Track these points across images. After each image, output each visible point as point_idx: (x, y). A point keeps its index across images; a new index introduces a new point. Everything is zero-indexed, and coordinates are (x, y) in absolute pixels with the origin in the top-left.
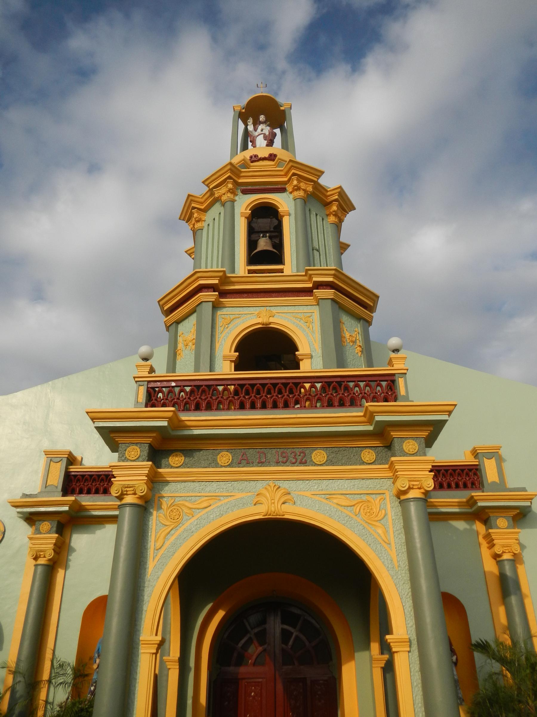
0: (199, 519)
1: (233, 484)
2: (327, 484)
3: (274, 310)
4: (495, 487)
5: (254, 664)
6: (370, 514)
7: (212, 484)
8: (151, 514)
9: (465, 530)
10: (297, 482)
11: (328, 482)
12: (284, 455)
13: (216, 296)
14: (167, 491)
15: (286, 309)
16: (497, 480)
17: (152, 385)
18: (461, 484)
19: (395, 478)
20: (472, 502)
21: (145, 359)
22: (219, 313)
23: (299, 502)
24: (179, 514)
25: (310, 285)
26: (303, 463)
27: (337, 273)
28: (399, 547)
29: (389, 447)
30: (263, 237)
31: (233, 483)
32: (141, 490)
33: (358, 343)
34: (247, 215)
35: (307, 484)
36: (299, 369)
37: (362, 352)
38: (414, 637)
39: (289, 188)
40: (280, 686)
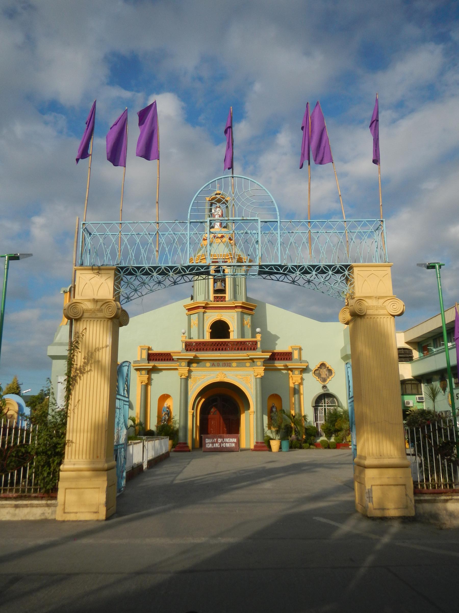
3: (223, 314)
4: (296, 361)
5: (213, 414)
8: (189, 380)
9: (286, 373)
14: (192, 374)
15: (226, 314)
16: (297, 358)
17: (186, 343)
18: (285, 358)
19: (254, 372)
20: (286, 366)
21: (184, 334)
22: (205, 314)
23: (228, 377)
25: (234, 306)
26: (230, 366)
29: (254, 362)
30: (219, 281)
33: (249, 324)
36: (230, 338)
37: (250, 327)
38: (255, 411)
39: (229, 262)
40: (222, 421)
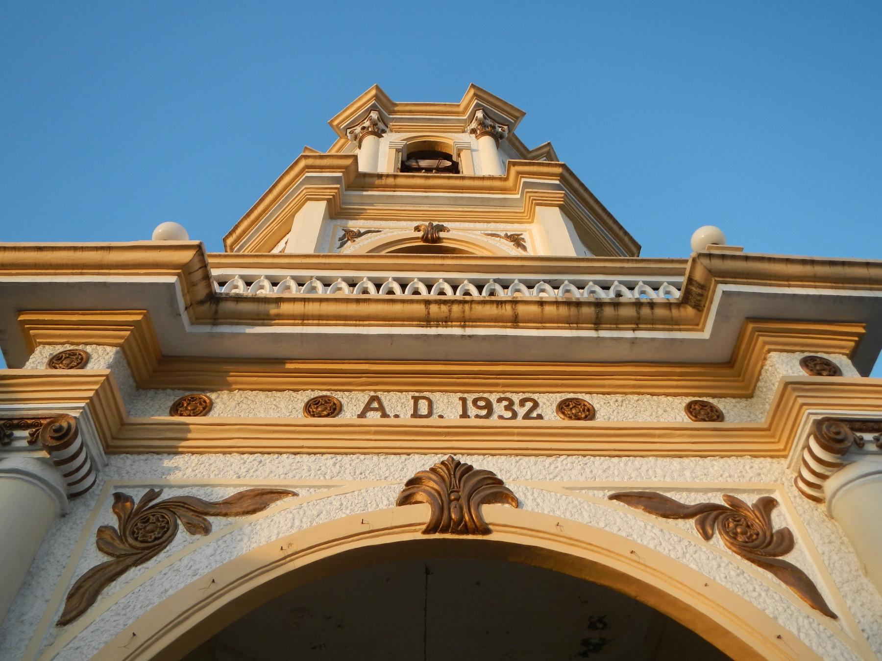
0: (225, 539)
1: (340, 461)
2: (605, 466)
6: (748, 538)
7: (277, 461)
10: (520, 460)
11: (606, 463)
12: (482, 403)
13: (336, 191)
24: (164, 527)
27: (567, 175)
28: (871, 629)
31: (339, 457)
32: (56, 431)
34: (400, 146)
35: (550, 464)
